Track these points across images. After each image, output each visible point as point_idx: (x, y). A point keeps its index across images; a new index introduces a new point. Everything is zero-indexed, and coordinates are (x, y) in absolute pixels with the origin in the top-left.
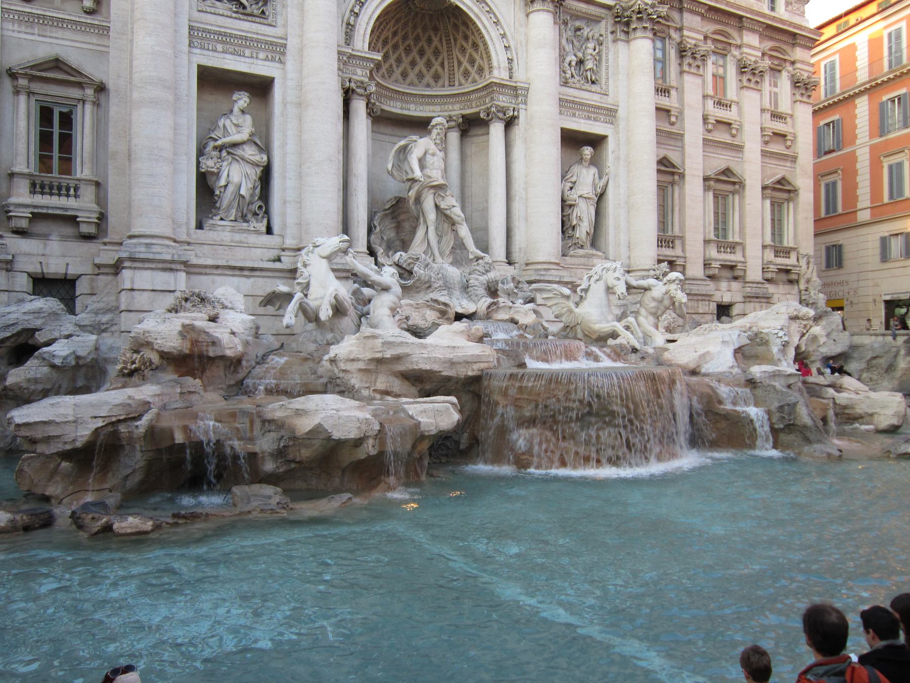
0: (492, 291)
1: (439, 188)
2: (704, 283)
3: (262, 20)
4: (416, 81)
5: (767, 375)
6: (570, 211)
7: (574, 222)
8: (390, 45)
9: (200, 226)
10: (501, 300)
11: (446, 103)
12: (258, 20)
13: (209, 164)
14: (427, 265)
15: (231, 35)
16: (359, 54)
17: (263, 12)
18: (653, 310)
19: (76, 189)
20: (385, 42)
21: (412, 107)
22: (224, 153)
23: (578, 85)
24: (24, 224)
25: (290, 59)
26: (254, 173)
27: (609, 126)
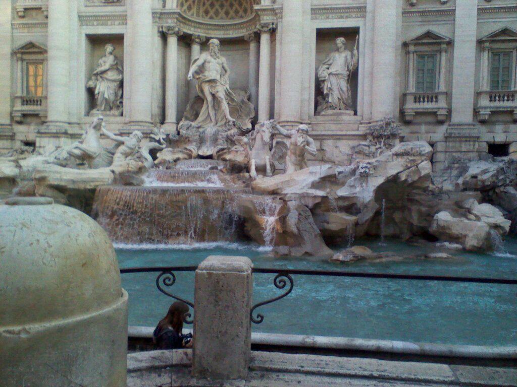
0: (231, 141)
1: (212, 82)
2: (472, 127)
3: (117, 4)
5: (297, 196)
6: (323, 85)
7: (325, 92)
9: (88, 114)
13: (91, 84)
14: (188, 128)
15: (99, 16)
18: (293, 151)
21: (231, 32)
22: (99, 77)
25: (129, 21)
26: (113, 86)
27: (360, 19)
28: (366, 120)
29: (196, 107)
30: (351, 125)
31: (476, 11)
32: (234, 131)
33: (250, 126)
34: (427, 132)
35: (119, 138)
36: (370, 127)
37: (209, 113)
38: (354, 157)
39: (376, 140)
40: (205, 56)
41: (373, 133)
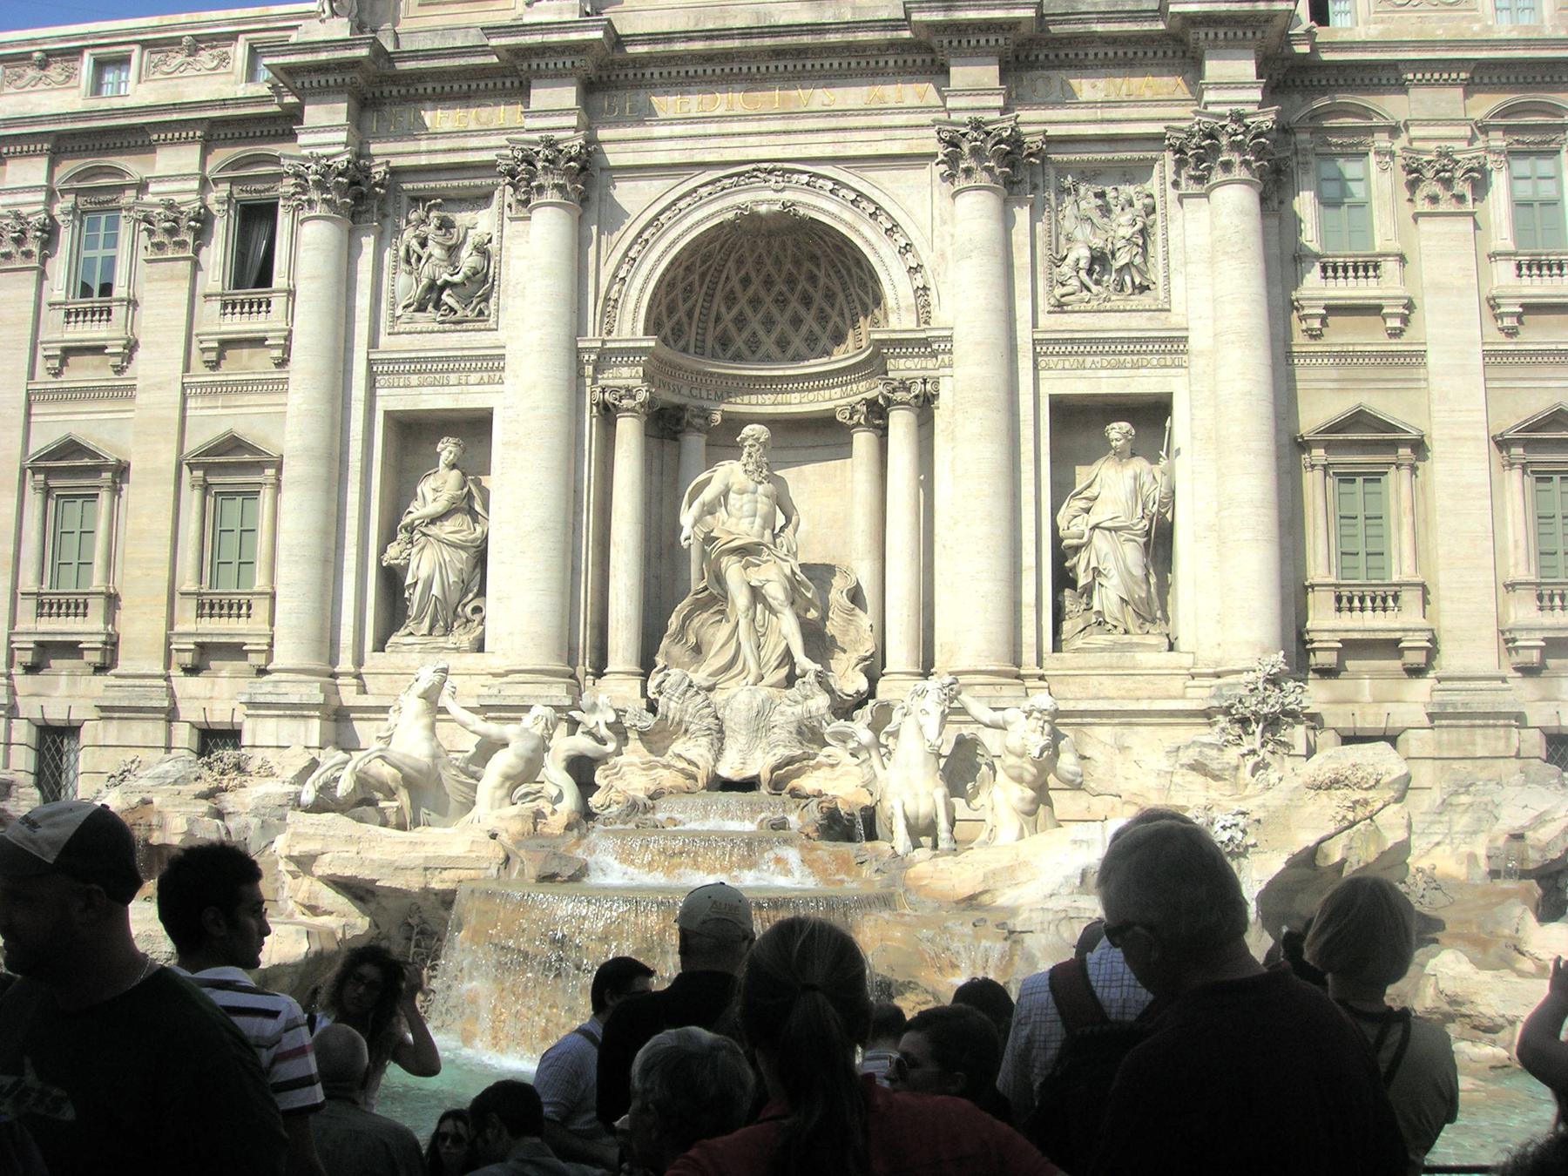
0: (810, 734)
2: (1498, 684)
4: (804, 350)
5: (1050, 916)
7: (1082, 581)
8: (743, 302)
9: (380, 646)
10: (827, 750)
11: (847, 384)
12: (470, 326)
15: (426, 360)
16: (617, 345)
17: (481, 313)
19: (249, 607)
20: (731, 299)
23: (1094, 303)
24: (187, 659)
28: (1207, 666)
29: (696, 622)
30: (1162, 682)
31: (1480, 362)
32: (821, 702)
33: (862, 684)
34: (1378, 701)
35: (493, 729)
36: (1219, 688)
37: (739, 644)
38: (1176, 779)
39: (1237, 729)
40: (730, 472)
41: (1232, 706)
